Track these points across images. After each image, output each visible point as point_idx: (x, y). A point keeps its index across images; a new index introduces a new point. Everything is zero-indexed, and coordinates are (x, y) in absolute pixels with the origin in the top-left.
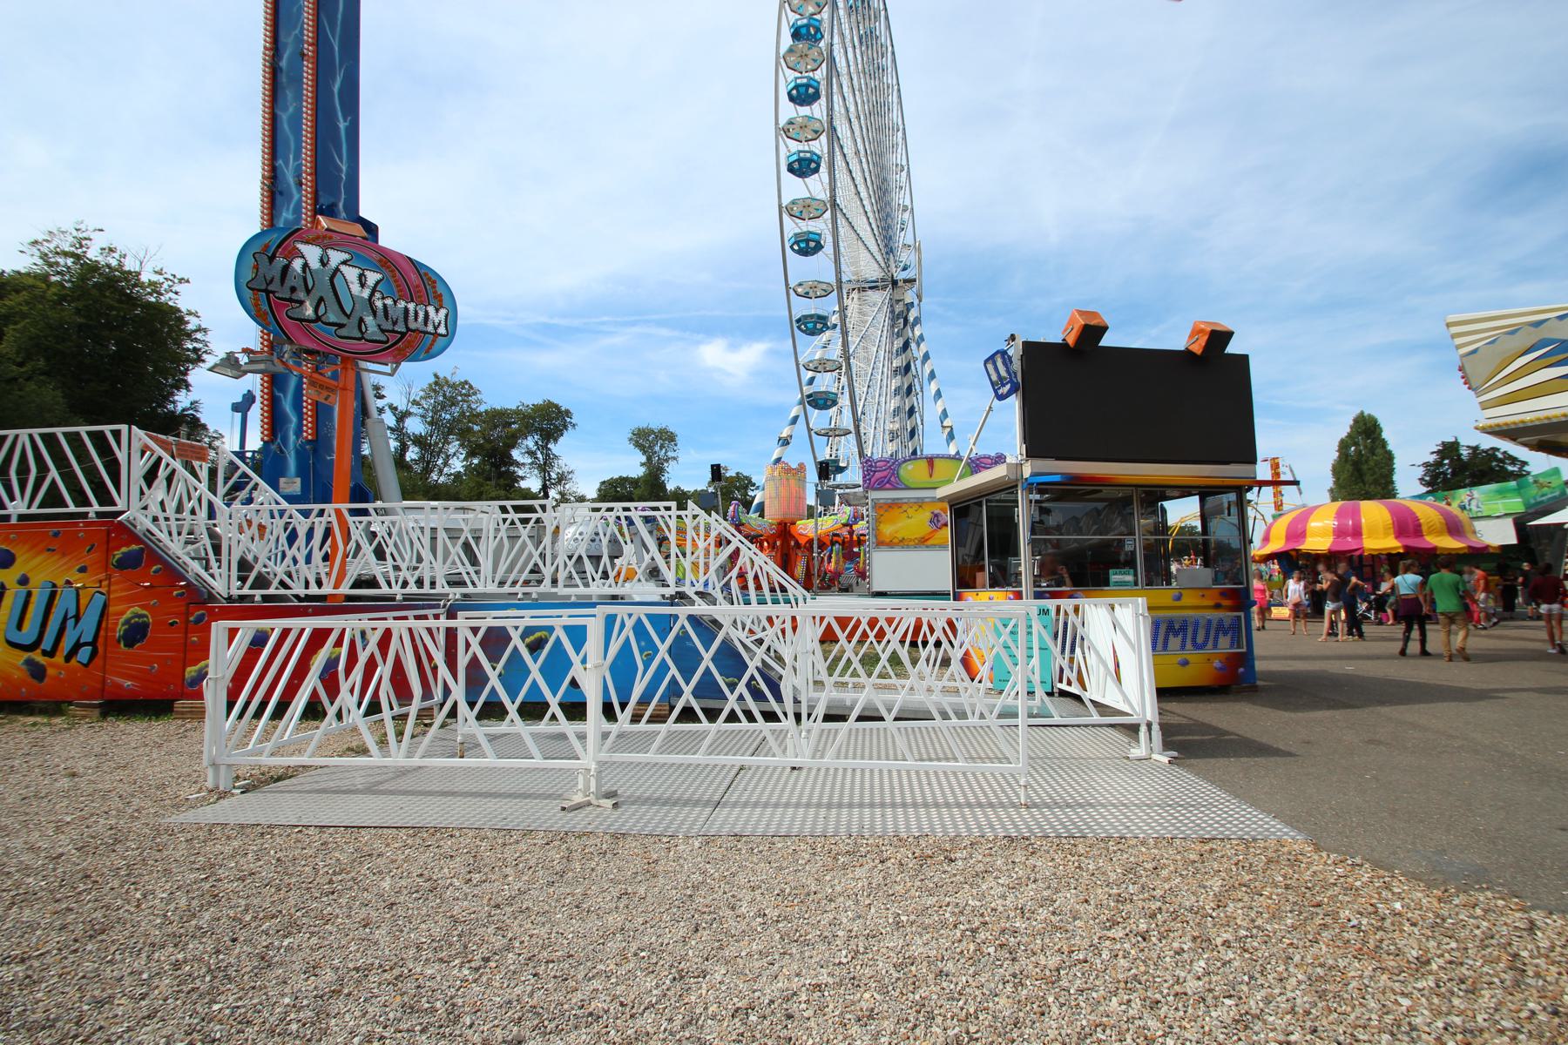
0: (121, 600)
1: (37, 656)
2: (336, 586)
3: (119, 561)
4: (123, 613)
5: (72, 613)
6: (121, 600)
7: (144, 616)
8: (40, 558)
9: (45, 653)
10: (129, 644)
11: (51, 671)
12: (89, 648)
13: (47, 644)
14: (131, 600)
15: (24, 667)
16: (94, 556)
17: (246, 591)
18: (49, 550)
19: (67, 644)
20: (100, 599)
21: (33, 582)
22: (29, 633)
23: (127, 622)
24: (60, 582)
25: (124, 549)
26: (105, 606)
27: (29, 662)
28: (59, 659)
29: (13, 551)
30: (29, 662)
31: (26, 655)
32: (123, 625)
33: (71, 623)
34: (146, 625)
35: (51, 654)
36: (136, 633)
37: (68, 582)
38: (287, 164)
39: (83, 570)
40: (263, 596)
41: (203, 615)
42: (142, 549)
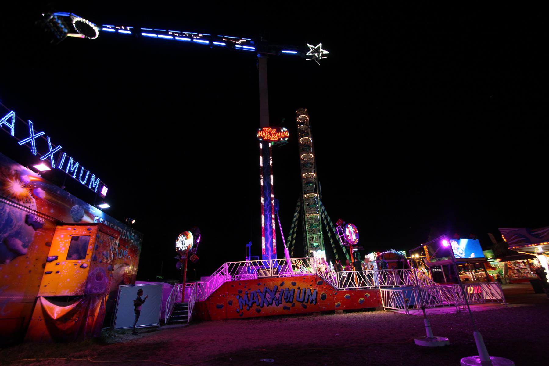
0: (320, 291)
1: (304, 303)
2: (359, 286)
3: (318, 283)
4: (320, 293)
5: (310, 294)
6: (320, 291)
7: (324, 294)
8: (301, 284)
9: (306, 303)
10: (323, 300)
11: (307, 306)
12: (315, 301)
13: (306, 301)
14: (322, 291)
15: (302, 306)
17: (342, 288)
18: (303, 282)
19: (310, 300)
20: (315, 291)
21: (301, 288)
22: (302, 298)
23: (322, 295)
24: (307, 288)
25: (319, 281)
26: (317, 292)
28: (309, 303)
29: (296, 282)
30: (303, 305)
31: (302, 303)
32: (321, 296)
33: (310, 296)
35: (307, 302)
36: (324, 297)
37: (308, 288)
38: (267, 192)
39: (311, 285)
40: (345, 289)
41: (336, 293)
42: (322, 281)
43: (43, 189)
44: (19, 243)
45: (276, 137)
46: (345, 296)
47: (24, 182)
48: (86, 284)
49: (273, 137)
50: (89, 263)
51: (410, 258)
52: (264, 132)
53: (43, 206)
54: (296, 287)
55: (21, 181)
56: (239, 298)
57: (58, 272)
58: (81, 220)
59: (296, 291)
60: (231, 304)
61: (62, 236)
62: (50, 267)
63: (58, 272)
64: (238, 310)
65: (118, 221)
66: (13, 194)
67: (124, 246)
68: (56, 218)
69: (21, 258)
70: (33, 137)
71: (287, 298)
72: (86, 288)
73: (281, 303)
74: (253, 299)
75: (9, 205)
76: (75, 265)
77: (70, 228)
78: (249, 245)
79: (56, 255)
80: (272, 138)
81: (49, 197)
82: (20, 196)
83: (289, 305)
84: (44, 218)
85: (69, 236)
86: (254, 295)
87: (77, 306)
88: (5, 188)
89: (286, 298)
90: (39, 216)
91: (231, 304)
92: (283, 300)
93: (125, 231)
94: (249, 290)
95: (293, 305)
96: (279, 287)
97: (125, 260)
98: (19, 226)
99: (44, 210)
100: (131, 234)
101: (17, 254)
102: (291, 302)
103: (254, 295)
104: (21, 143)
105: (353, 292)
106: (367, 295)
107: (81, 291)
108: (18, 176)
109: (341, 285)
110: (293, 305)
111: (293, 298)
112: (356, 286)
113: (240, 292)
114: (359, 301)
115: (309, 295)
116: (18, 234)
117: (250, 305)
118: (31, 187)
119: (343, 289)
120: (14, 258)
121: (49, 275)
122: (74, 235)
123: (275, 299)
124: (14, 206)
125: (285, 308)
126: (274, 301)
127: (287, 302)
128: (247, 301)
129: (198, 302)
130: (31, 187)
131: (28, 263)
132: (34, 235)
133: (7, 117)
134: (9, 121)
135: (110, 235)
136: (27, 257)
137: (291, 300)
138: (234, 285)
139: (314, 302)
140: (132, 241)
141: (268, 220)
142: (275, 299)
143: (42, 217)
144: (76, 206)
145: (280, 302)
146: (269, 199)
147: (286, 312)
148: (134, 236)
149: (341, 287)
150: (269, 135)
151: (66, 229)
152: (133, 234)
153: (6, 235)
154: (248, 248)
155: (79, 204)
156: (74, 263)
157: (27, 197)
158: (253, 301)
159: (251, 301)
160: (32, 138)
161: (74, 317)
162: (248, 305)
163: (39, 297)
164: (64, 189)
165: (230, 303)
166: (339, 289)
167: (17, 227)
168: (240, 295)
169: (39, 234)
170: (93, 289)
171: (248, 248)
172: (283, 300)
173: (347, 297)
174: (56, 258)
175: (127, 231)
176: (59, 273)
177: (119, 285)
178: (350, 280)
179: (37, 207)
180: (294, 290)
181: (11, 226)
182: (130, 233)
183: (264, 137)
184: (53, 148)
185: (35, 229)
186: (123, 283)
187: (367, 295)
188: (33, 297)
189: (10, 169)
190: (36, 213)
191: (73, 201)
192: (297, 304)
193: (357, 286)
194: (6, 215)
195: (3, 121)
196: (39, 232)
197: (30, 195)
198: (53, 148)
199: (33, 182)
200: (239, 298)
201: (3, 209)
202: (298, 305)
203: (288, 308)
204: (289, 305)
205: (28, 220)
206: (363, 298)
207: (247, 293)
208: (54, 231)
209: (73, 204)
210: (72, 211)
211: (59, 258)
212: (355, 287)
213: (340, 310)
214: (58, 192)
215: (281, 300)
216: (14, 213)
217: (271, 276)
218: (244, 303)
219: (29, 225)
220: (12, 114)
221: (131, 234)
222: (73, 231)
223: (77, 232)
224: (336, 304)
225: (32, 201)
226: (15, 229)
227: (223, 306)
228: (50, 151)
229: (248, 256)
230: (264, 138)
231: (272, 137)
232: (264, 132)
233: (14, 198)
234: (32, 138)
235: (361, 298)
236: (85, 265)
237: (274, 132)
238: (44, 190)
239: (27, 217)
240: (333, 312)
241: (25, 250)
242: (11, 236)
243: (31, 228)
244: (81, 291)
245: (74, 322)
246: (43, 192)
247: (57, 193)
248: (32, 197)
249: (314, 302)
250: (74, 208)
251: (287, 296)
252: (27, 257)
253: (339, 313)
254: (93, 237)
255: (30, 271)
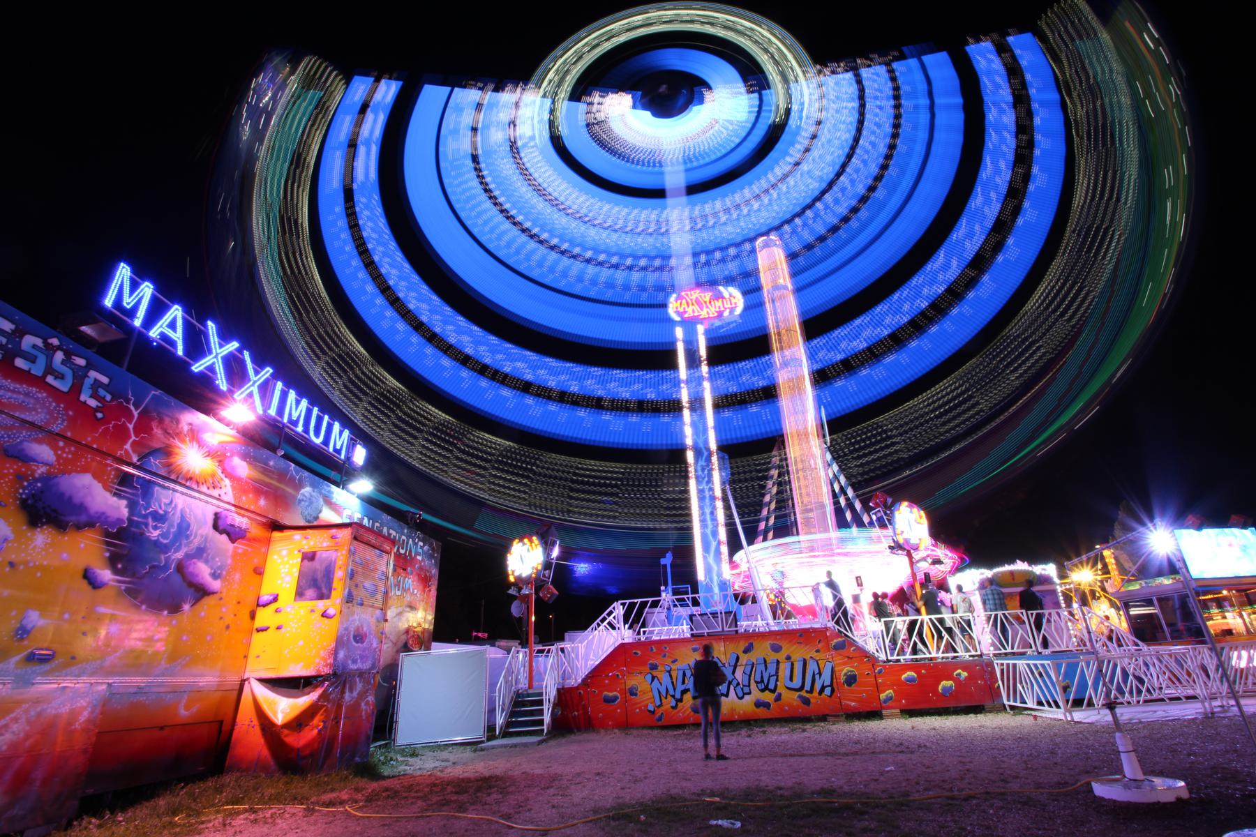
1: (803, 693)
4: (842, 671)
5: (817, 671)
8: (795, 647)
9: (807, 692)
10: (850, 684)
11: (812, 700)
13: (807, 687)
14: (845, 664)
16: (820, 645)
17: (895, 657)
19: (818, 686)
20: (829, 666)
21: (793, 658)
22: (797, 682)
23: (845, 674)
24: (807, 658)
27: (800, 697)
28: (815, 694)
30: (800, 697)
31: (798, 693)
33: (817, 677)
34: (855, 676)
35: (811, 691)
36: (851, 680)
39: (817, 651)
43: (245, 457)
44: (203, 571)
45: (713, 309)
46: (904, 676)
47: (208, 447)
48: (335, 652)
49: (705, 310)
50: (338, 608)
51: (1134, 611)
52: (684, 301)
53: (244, 492)
54: (781, 656)
55: (201, 444)
56: (653, 680)
57: (279, 628)
58: (317, 518)
59: (782, 666)
60: (636, 695)
61: (284, 553)
62: (265, 617)
63: (279, 628)
64: (651, 707)
65: (389, 517)
66: (188, 471)
67: (405, 570)
68: (270, 516)
69: (208, 602)
70: (217, 354)
71: (762, 681)
72: (335, 659)
73: (750, 693)
74: (683, 682)
75: (183, 493)
76: (313, 611)
77: (297, 535)
78: (667, 560)
79: (276, 592)
80: (704, 314)
81: (256, 474)
82: (200, 475)
83: (768, 697)
84: (248, 517)
85: (296, 552)
86: (684, 675)
87: (321, 697)
88: (172, 460)
89: (759, 680)
90: (239, 514)
91: (636, 695)
92: (753, 684)
93: (404, 537)
94: (674, 662)
95: (778, 698)
96: (742, 656)
97: (408, 598)
98: (202, 536)
99: (247, 500)
100: (416, 544)
101: (202, 592)
102: (773, 691)
103: (684, 675)
104: (197, 367)
105: (924, 666)
106: (959, 674)
107: (326, 666)
108: (195, 435)
109: (892, 650)
110: (778, 698)
111: (777, 680)
112: (930, 653)
113: (654, 667)
114: (940, 688)
115: (814, 675)
116: (200, 553)
117: (678, 696)
118: (220, 456)
119: (898, 661)
120: (197, 600)
121: (264, 633)
122: (306, 549)
123: (735, 683)
124: (190, 496)
125: (758, 704)
126: (732, 687)
127: (762, 691)
128: (671, 691)
129: (563, 688)
130: (220, 456)
131: (224, 610)
132: (230, 553)
133: (168, 318)
134: (172, 325)
135: (375, 547)
136: (221, 599)
137: (771, 686)
138: (639, 652)
139: (828, 691)
140: (419, 558)
141: (707, 501)
142: (735, 683)
143: (243, 516)
144: (307, 490)
145: (746, 690)
146: (706, 454)
147: (762, 712)
148: (422, 547)
149: (892, 654)
150: (696, 307)
151: (290, 538)
152: (421, 543)
153: (179, 555)
154: (665, 566)
155: (313, 486)
156: (309, 608)
157: (213, 476)
158: (683, 687)
159: (680, 687)
160: (216, 357)
161: (315, 721)
162: (673, 696)
163: (248, 679)
164: (282, 456)
165: (633, 692)
166: (888, 661)
167: (198, 538)
168: (655, 673)
169: (240, 551)
170: (350, 662)
171: (665, 566)
172: (753, 684)
173: (910, 680)
174: (275, 599)
175: (409, 537)
176: (283, 630)
177: (398, 652)
178: (914, 638)
179: (234, 495)
180: (778, 662)
181: (188, 537)
182: (414, 541)
183: (685, 312)
184: (257, 373)
185: (233, 540)
186: (406, 648)
187: (959, 674)
188: (236, 679)
189: (178, 421)
190: (233, 508)
191: (300, 479)
192: (788, 696)
193: (933, 652)
194: (178, 514)
195: (161, 326)
196: (240, 546)
197: (219, 471)
198: (257, 373)
199: (222, 444)
200: (653, 680)
201: (171, 502)
202: (791, 698)
203: (767, 705)
204: (768, 697)
205: (218, 524)
206: (950, 683)
207: (668, 669)
208: (268, 542)
209: (299, 486)
210: (300, 501)
211: (279, 598)
212: (928, 656)
213: (893, 711)
214: (271, 463)
215: (749, 686)
216: (191, 510)
217: (720, 629)
218: (664, 693)
219: (221, 533)
220: (176, 312)
221: (416, 544)
222: (304, 542)
223: (312, 543)
224: (883, 696)
225: (223, 484)
226: (196, 542)
227: (615, 698)
228: (249, 380)
229: (666, 585)
230: (686, 316)
231: (702, 309)
232: (684, 301)
233: (188, 481)
234: (216, 357)
235: (944, 683)
236: (331, 612)
237: (707, 299)
238: (245, 460)
239: (217, 516)
240: (875, 714)
241: (215, 585)
242: (189, 556)
243: (224, 537)
244: (326, 666)
245: (316, 731)
246: (244, 464)
247: (268, 465)
248: (223, 476)
249: (828, 691)
250: (304, 495)
251: (762, 677)
252: (221, 599)
253: (892, 716)
254: (344, 552)
255: (228, 627)
